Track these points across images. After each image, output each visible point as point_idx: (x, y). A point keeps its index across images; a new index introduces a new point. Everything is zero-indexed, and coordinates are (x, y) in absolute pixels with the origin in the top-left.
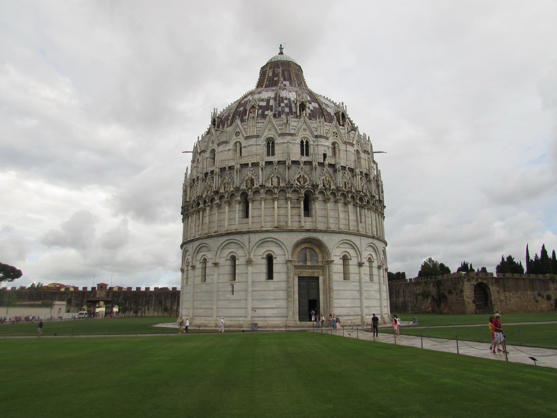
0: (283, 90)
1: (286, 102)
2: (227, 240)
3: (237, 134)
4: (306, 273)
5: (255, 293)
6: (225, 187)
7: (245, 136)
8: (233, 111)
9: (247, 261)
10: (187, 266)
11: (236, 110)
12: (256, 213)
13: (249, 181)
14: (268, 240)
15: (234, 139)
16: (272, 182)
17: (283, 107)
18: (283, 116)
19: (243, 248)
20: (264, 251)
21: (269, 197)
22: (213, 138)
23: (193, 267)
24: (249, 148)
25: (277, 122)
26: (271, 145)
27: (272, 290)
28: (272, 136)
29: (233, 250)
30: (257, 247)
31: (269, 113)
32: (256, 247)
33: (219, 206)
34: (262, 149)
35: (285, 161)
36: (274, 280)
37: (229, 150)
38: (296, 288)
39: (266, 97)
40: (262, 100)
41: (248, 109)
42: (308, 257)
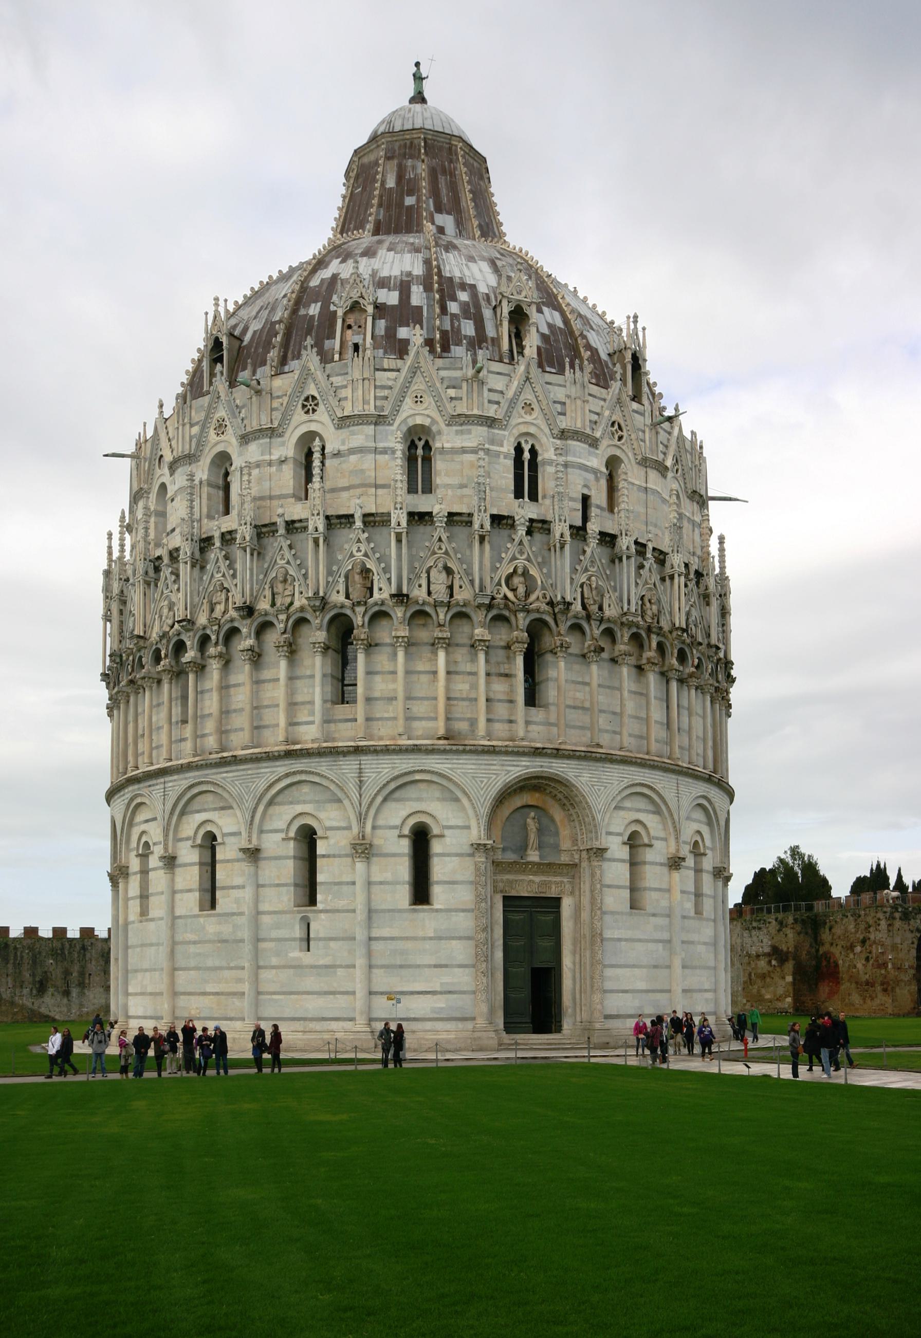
4: (528, 885)
5: (377, 946)
7: (340, 415)
9: (354, 846)
12: (381, 686)
13: (357, 578)
20: (404, 813)
21: (424, 635)
24: (353, 458)
26: (419, 453)
27: (431, 938)
29: (307, 808)
30: (385, 800)
32: (380, 799)
34: (394, 468)
36: (436, 906)
38: (499, 932)
42: (532, 837)
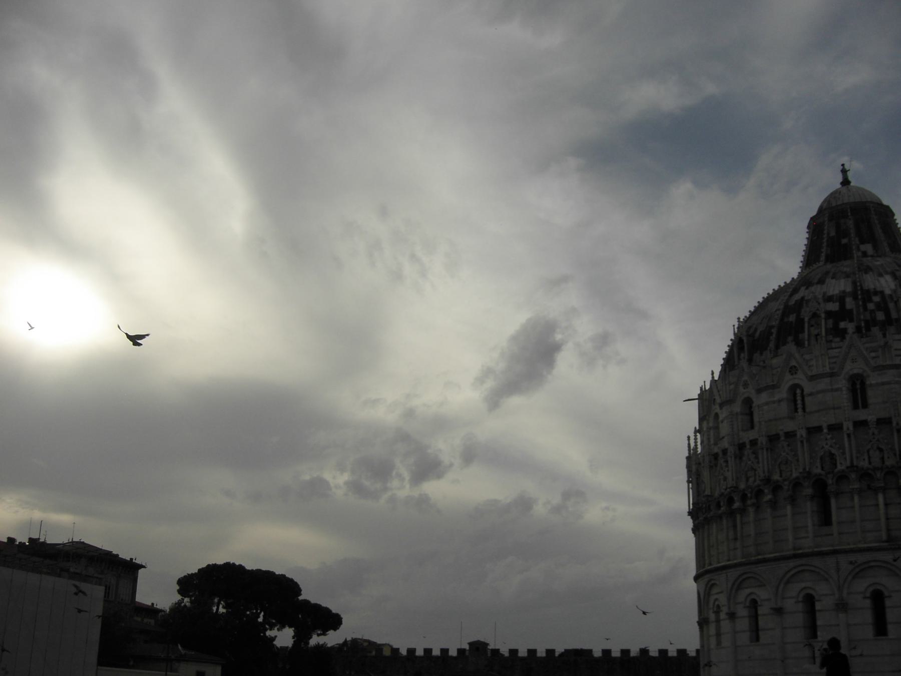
0: (866, 273)
1: (876, 299)
2: (795, 567)
3: (793, 370)
6: (781, 471)
7: (810, 374)
8: (775, 323)
10: (717, 612)
11: (782, 320)
14: (872, 564)
15: (789, 380)
16: (869, 458)
17: (872, 311)
18: (875, 330)
19: (827, 580)
22: (746, 378)
23: (732, 616)
25: (867, 345)
28: (860, 371)
31: (850, 327)
33: (774, 504)
34: (844, 398)
35: (890, 418)
37: (780, 401)
39: (836, 292)
40: (829, 299)
41: (806, 319)
